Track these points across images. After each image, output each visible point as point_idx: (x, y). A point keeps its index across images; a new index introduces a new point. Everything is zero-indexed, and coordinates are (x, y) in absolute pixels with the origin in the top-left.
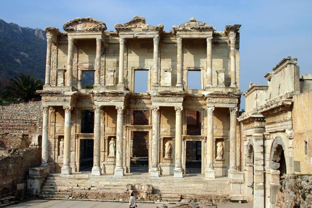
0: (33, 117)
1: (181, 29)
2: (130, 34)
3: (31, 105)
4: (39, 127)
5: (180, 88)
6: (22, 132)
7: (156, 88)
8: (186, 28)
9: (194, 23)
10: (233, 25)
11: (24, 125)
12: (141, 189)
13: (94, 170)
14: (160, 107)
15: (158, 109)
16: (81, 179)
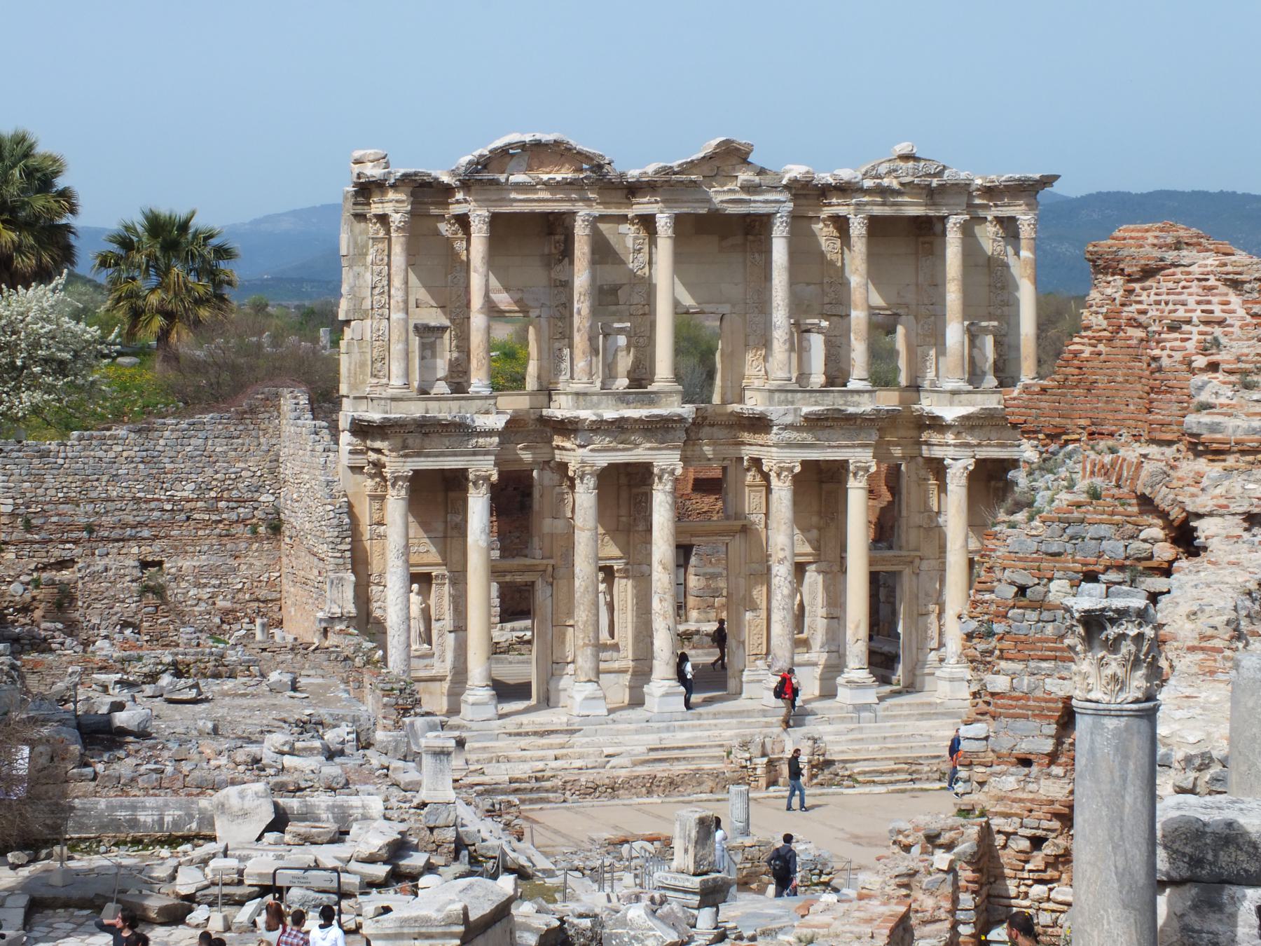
0: (178, 486)
1: (868, 183)
2: (697, 201)
3: (167, 434)
4: (340, 547)
5: (867, 395)
6: (135, 550)
7: (790, 395)
8: (886, 182)
9: (911, 164)
10: (1037, 176)
11: (139, 523)
12: (783, 751)
13: (586, 699)
14: (804, 463)
15: (798, 469)
16: (552, 732)
